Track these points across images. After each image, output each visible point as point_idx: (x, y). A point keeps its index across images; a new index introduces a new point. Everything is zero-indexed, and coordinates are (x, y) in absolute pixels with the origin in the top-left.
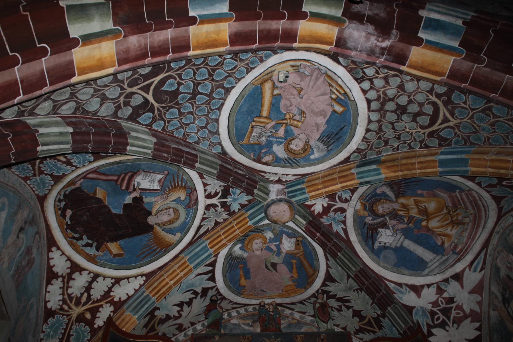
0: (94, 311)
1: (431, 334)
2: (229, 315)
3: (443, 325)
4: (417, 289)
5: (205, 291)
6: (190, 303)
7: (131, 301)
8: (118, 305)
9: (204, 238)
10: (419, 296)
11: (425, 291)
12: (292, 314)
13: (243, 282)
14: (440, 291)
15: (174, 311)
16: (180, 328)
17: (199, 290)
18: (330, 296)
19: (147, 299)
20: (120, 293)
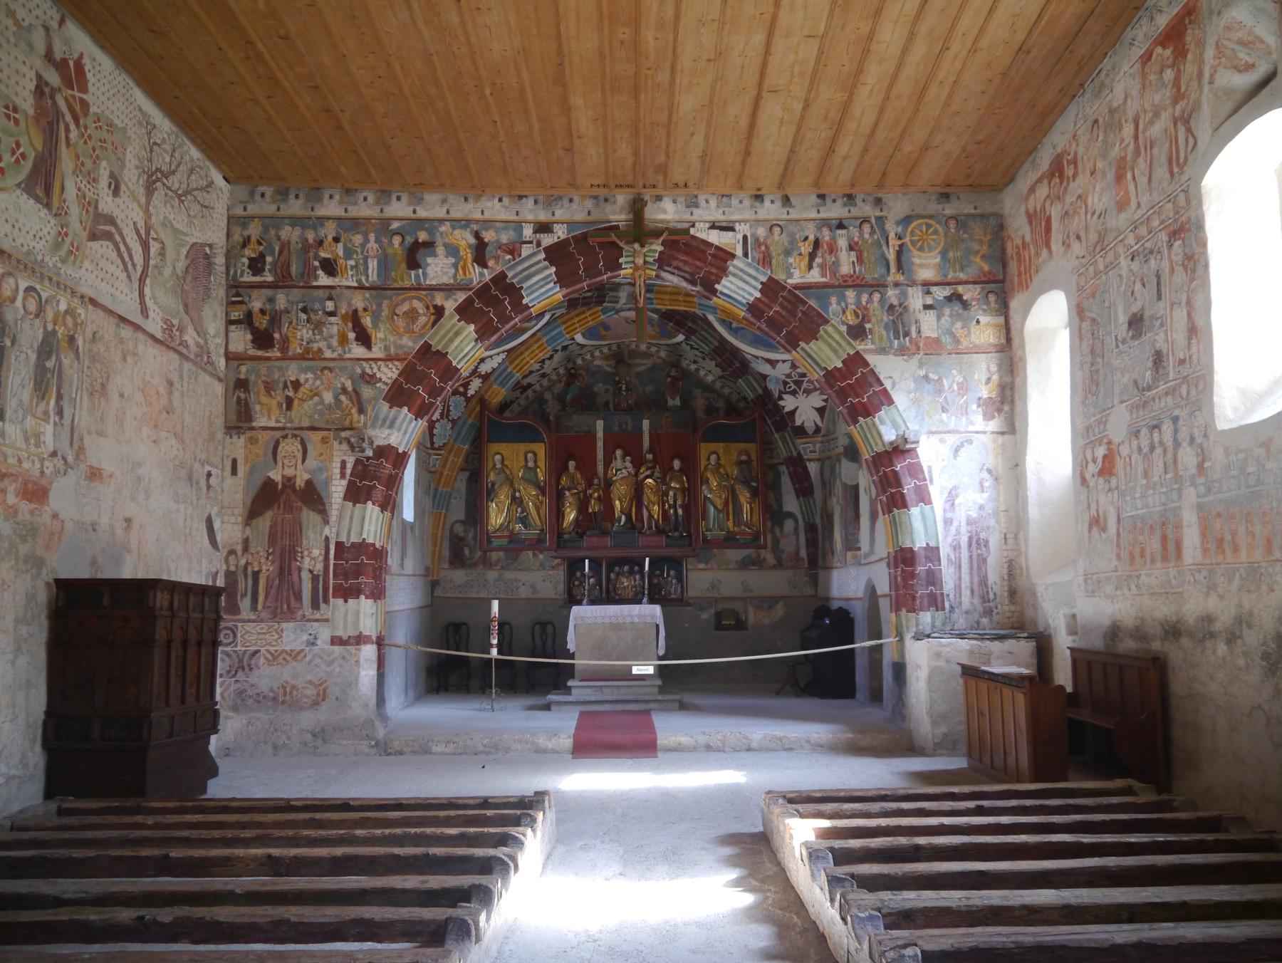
0: (466, 386)
1: (781, 398)
2: (592, 355)
3: (794, 393)
4: (773, 363)
5: (565, 348)
6: (551, 357)
7: (496, 374)
8: (485, 377)
9: (559, 321)
10: (774, 367)
11: (780, 365)
12: (658, 352)
13: (603, 333)
14: (794, 366)
15: (537, 366)
16: (543, 375)
17: (559, 348)
18: (692, 348)
19: (511, 375)
20: (485, 368)
